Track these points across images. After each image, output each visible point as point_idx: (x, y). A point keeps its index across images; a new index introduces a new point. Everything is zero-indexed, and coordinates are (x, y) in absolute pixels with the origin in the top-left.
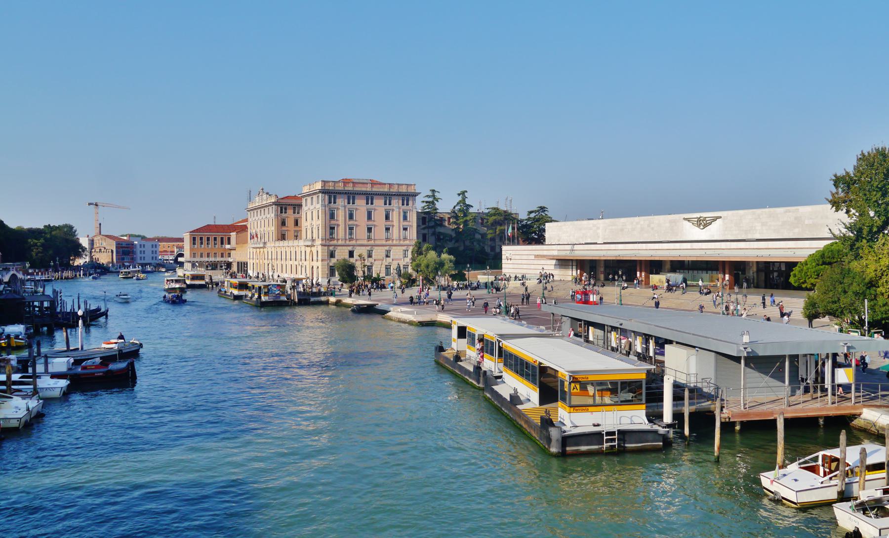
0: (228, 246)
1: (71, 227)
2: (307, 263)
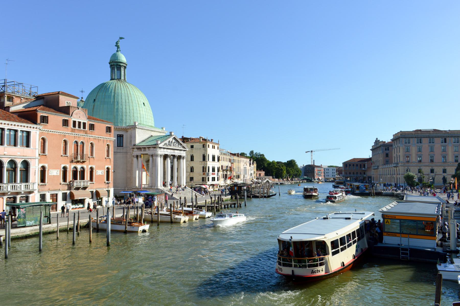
1: (294, 161)
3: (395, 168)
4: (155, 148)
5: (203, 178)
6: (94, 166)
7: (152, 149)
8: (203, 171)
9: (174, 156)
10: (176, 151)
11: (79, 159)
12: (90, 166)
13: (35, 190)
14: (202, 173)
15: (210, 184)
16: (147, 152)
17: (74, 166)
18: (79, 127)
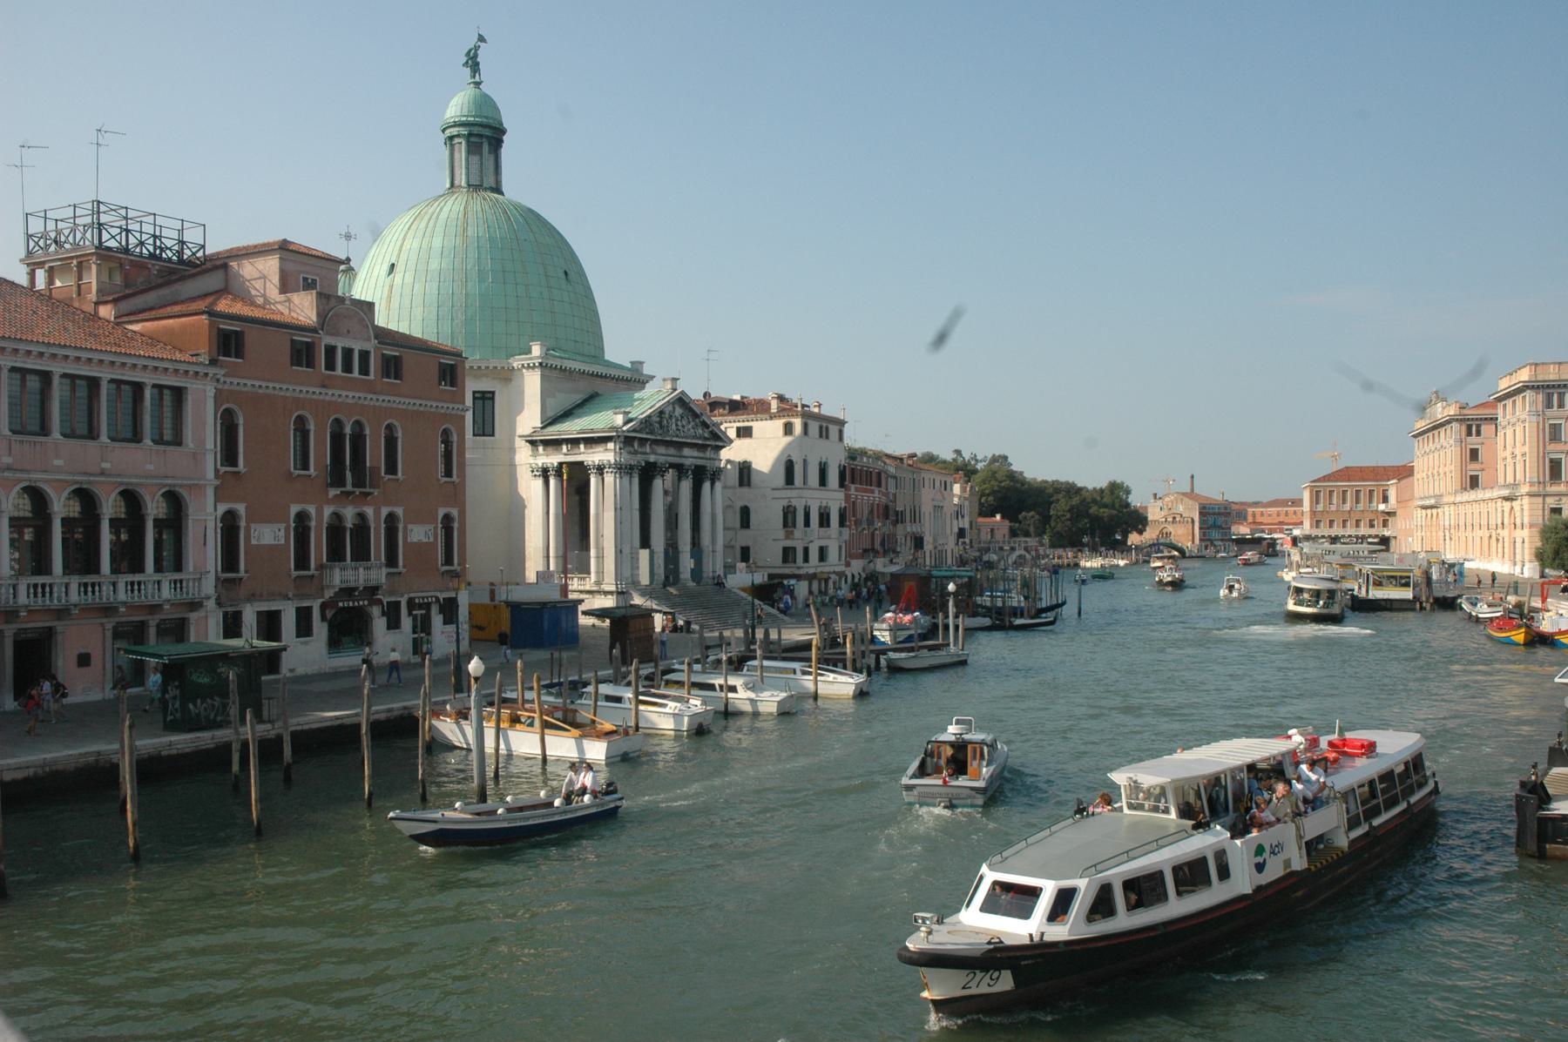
0: (1382, 507)
2: (1505, 533)
3: (1507, 505)
5: (786, 550)
6: (399, 511)
8: (785, 525)
9: (680, 469)
10: (687, 452)
11: (349, 487)
12: (385, 511)
13: (208, 598)
14: (781, 533)
15: (812, 571)
18: (348, 367)
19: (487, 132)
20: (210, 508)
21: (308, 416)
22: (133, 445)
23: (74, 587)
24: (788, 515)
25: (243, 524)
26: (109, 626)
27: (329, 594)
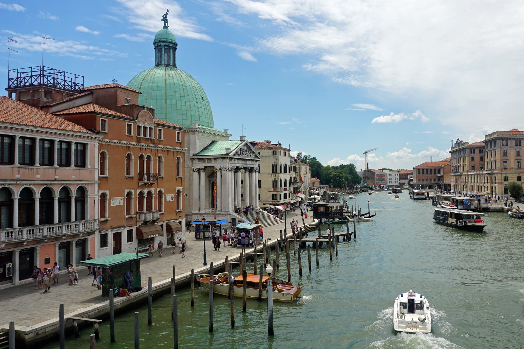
1: (353, 165)
4: (224, 158)
5: (273, 195)
6: (163, 190)
7: (219, 161)
8: (273, 187)
9: (245, 168)
10: (248, 162)
11: (146, 182)
12: (158, 190)
15: (282, 202)
16: (213, 164)
17: (140, 190)
19: (171, 45)
20: (96, 193)
21: (132, 154)
22: (67, 168)
23: (45, 230)
24: (275, 183)
25: (108, 198)
26: (57, 245)
27: (139, 224)
